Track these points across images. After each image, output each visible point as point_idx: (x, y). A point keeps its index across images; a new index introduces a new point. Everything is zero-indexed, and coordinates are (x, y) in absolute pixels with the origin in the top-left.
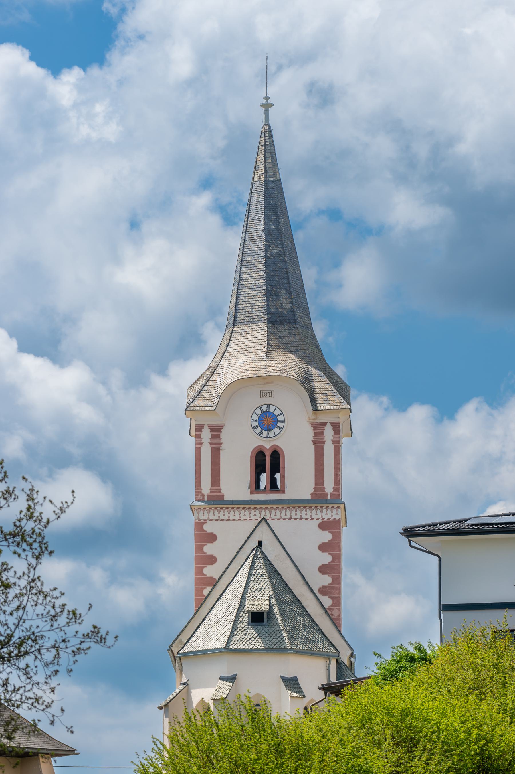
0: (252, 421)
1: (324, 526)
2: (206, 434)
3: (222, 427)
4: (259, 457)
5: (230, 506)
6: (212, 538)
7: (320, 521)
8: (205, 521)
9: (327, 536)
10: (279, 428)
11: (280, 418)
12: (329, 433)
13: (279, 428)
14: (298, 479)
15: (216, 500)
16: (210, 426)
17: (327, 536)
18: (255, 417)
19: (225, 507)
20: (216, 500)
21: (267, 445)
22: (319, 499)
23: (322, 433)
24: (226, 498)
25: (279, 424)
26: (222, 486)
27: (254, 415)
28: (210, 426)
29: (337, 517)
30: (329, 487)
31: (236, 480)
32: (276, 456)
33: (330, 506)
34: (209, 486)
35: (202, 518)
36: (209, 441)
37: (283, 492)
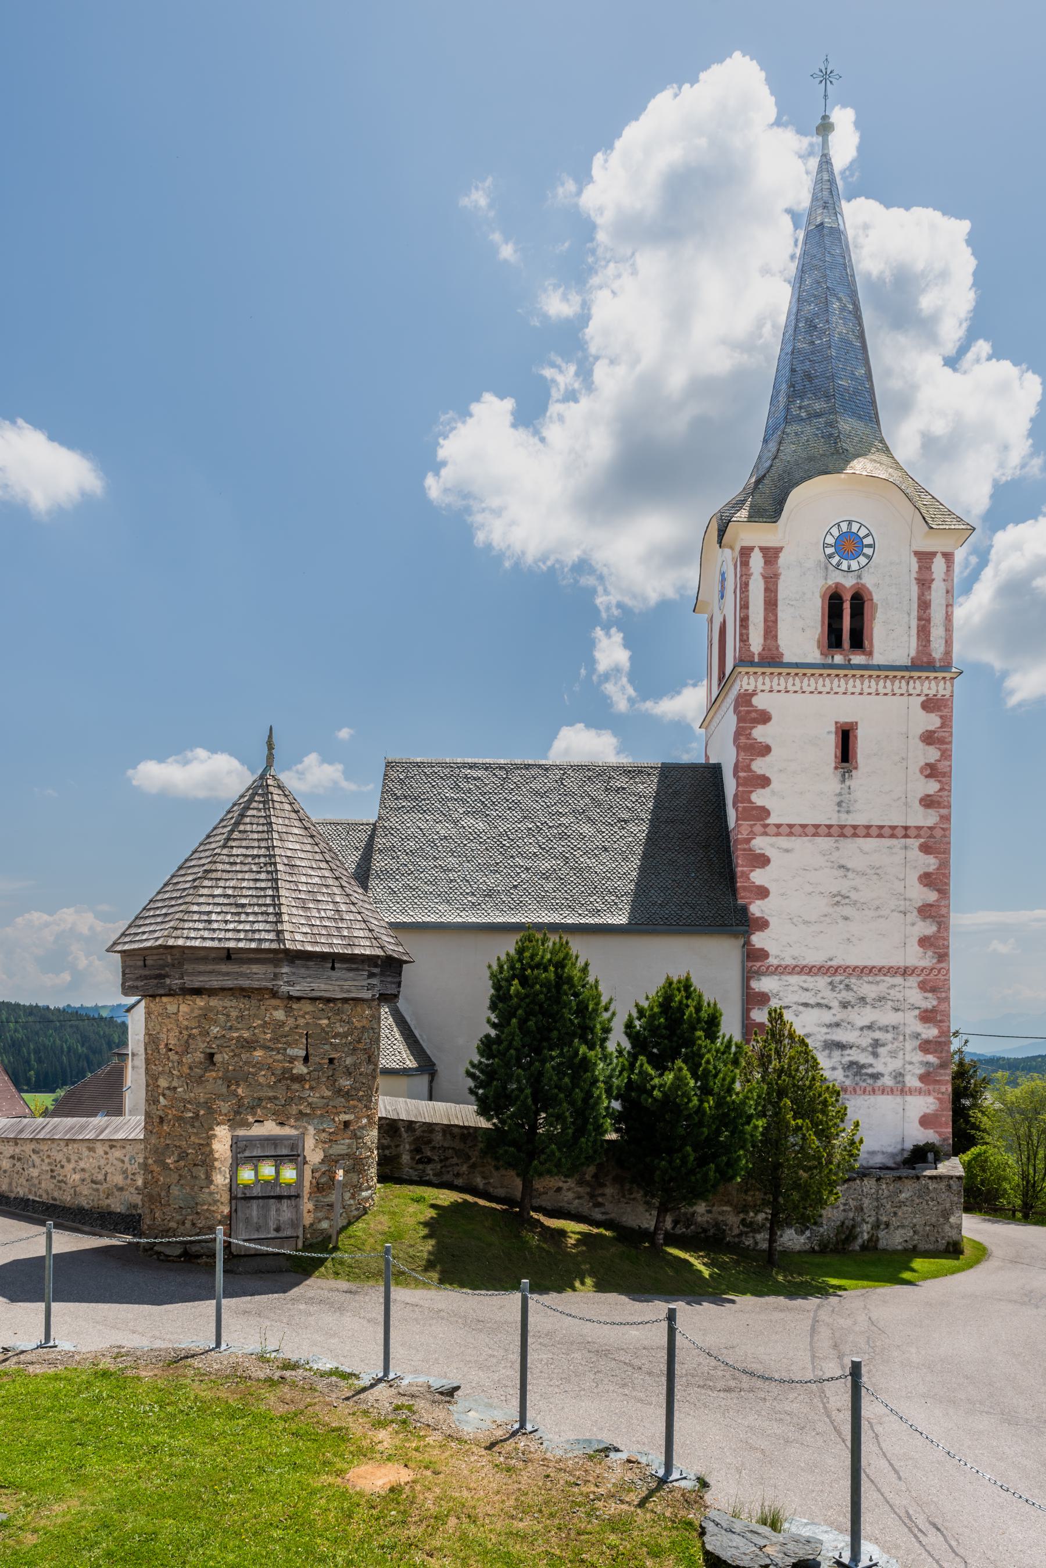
0: (825, 545)
1: (930, 705)
2: (757, 561)
3: (779, 550)
4: (834, 602)
5: (793, 671)
6: (764, 718)
7: (923, 698)
8: (754, 693)
9: (933, 721)
10: (865, 555)
11: (868, 541)
12: (938, 565)
13: (865, 555)
14: (891, 637)
15: (771, 660)
16: (762, 549)
17: (933, 721)
18: (830, 540)
19: (785, 671)
20: (771, 660)
21: (849, 582)
22: (923, 664)
23: (929, 568)
24: (786, 659)
25: (866, 550)
26: (780, 642)
27: (829, 537)
28: (762, 549)
29: (948, 693)
30: (937, 650)
31: (801, 634)
32: (860, 601)
33: (940, 675)
34: (761, 641)
35: (751, 688)
36: (761, 570)
37: (870, 654)
